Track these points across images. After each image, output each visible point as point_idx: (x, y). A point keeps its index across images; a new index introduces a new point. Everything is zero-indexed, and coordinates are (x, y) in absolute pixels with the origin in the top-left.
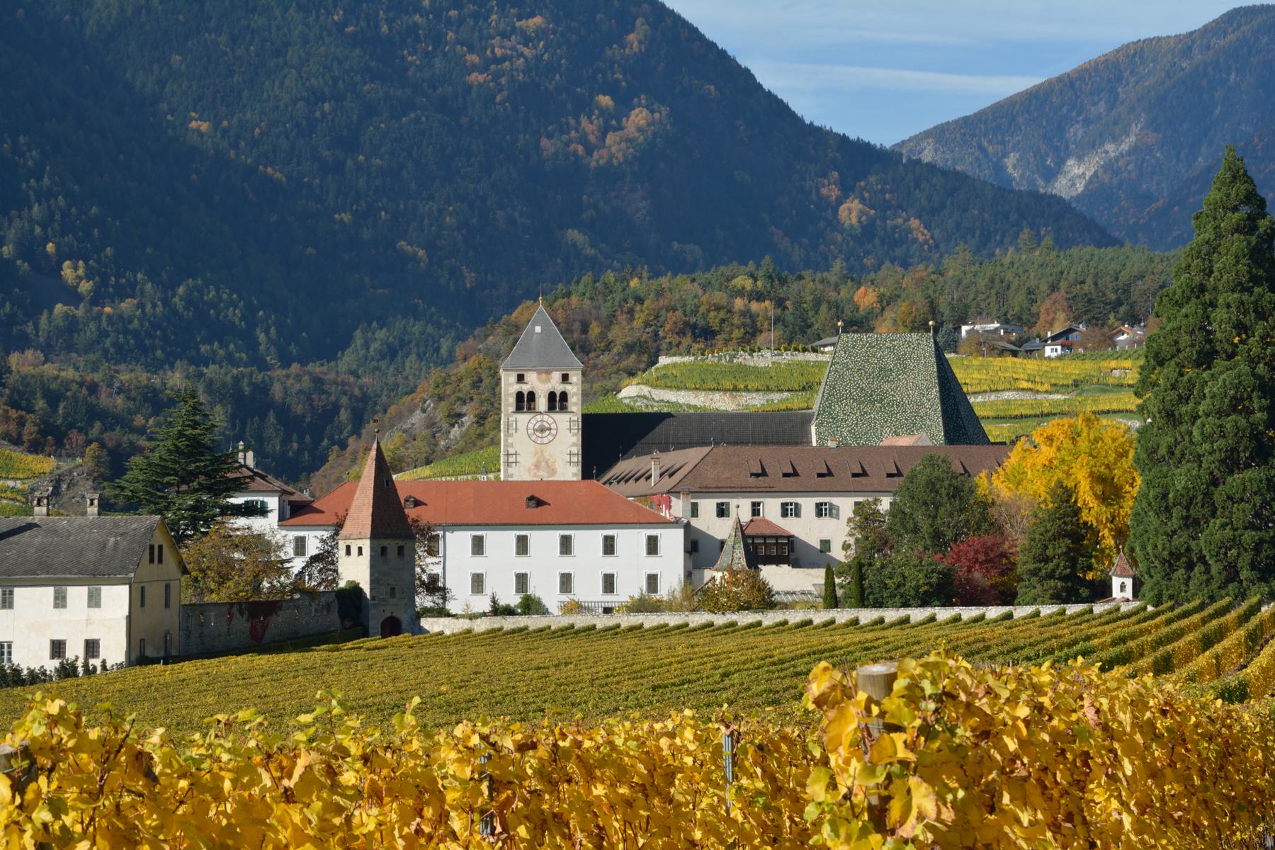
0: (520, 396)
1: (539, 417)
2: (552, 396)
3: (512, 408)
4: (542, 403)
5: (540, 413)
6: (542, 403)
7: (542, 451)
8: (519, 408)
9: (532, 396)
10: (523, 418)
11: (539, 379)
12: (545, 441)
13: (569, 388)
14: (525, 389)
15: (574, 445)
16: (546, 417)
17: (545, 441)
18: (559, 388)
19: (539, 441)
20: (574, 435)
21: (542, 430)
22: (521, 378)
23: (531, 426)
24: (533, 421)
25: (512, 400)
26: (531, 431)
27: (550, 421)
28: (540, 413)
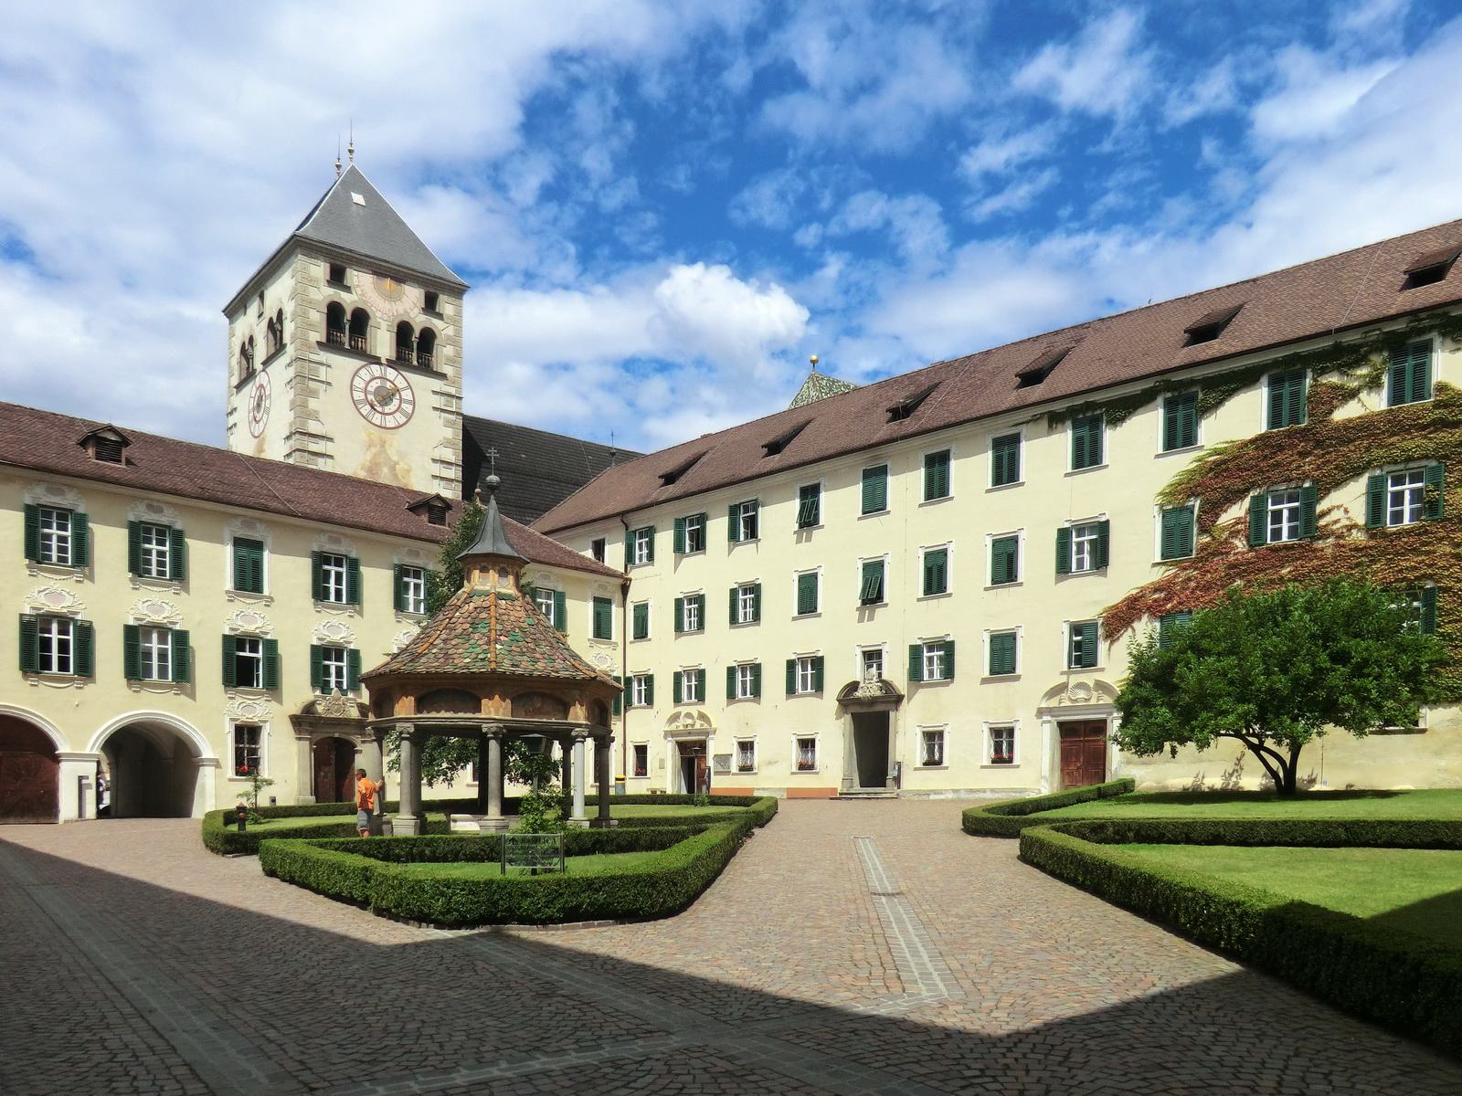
0: (334, 311)
1: (375, 368)
2: (403, 330)
3: (319, 335)
4: (382, 341)
5: (377, 361)
6: (382, 341)
7: (383, 443)
8: (331, 344)
9: (361, 319)
10: (341, 366)
11: (377, 288)
12: (390, 422)
13: (436, 324)
14: (349, 301)
15: (447, 443)
16: (391, 373)
17: (390, 422)
18: (419, 320)
19: (377, 419)
20: (448, 424)
21: (385, 397)
22: (337, 277)
23: (359, 383)
24: (363, 373)
25: (318, 317)
26: (359, 396)
27: (400, 383)
28: (377, 361)
